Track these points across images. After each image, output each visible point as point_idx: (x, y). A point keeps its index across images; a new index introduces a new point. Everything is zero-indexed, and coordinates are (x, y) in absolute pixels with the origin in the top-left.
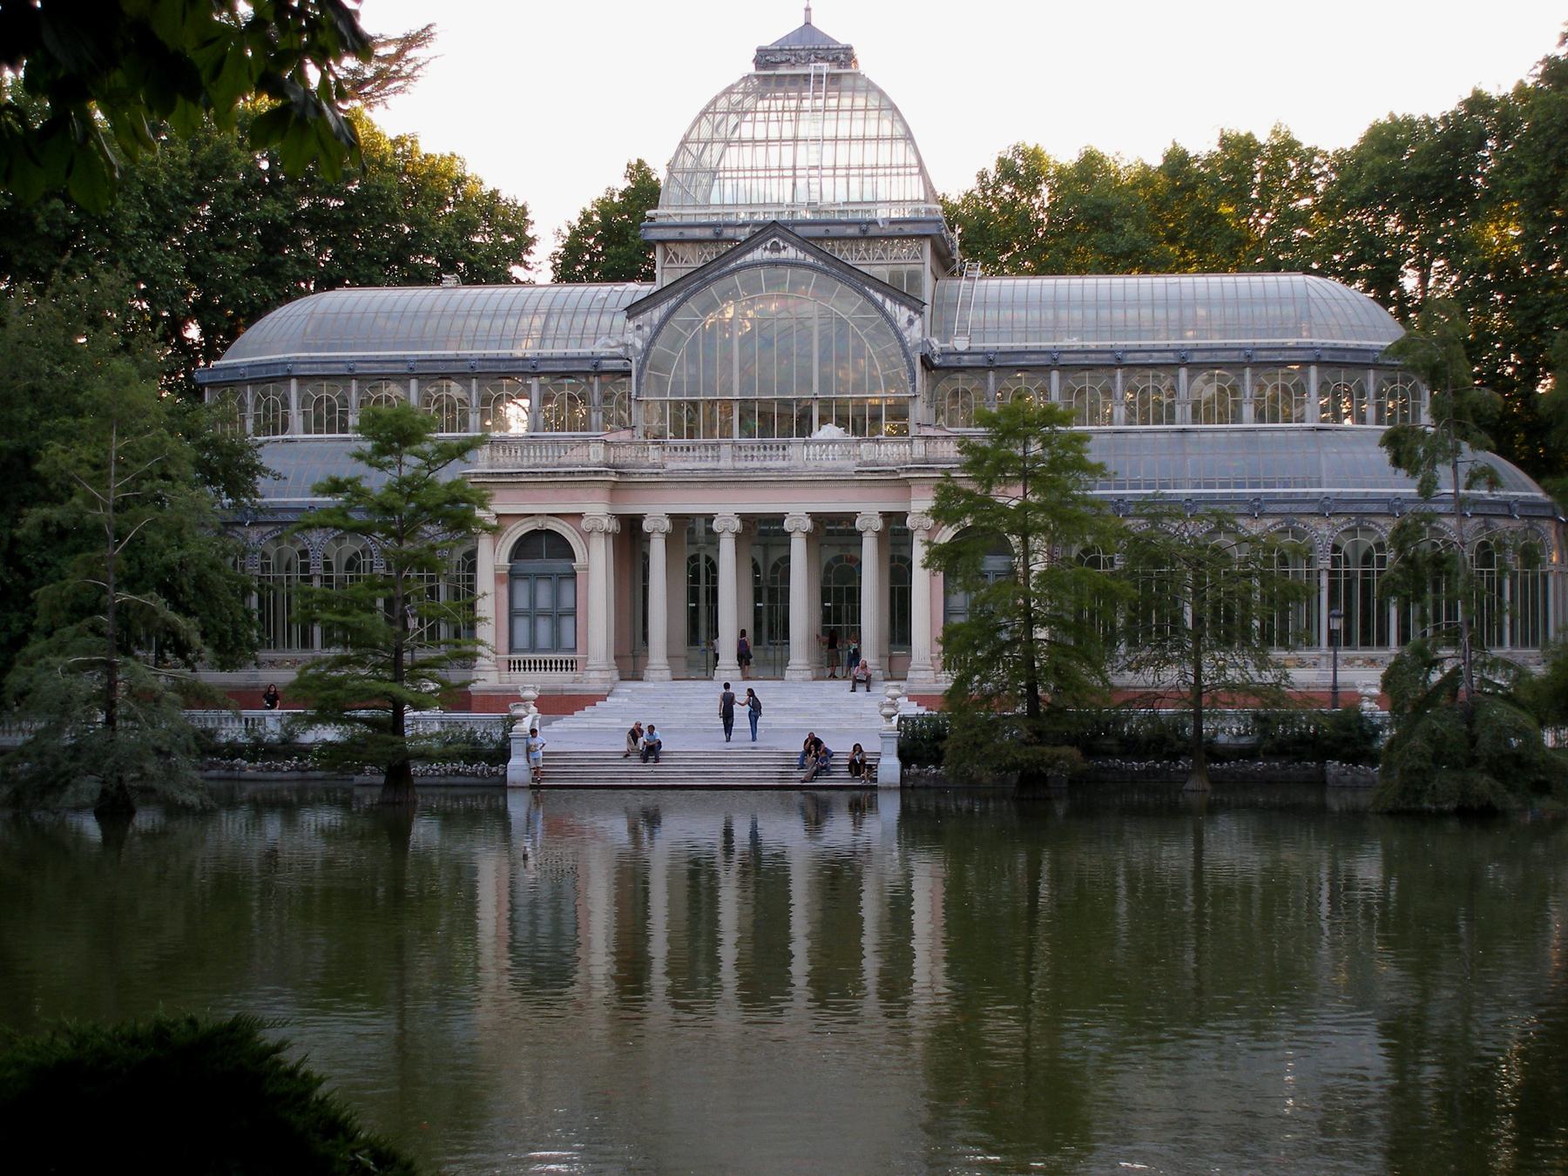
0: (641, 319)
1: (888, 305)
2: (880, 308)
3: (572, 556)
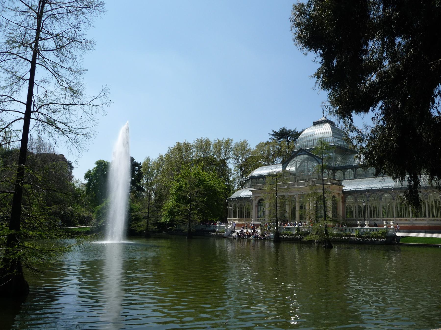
1: (318, 159)
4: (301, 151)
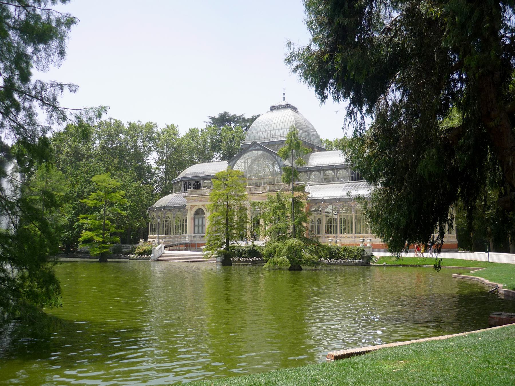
1: (276, 157)
2: (275, 158)
3: (204, 214)
4: (254, 145)
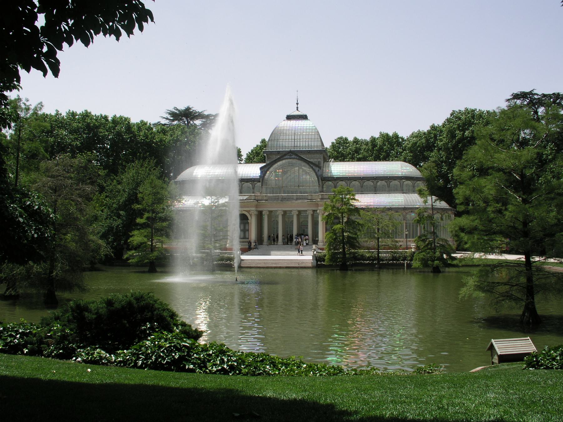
0: (263, 170)
1: (314, 167)
